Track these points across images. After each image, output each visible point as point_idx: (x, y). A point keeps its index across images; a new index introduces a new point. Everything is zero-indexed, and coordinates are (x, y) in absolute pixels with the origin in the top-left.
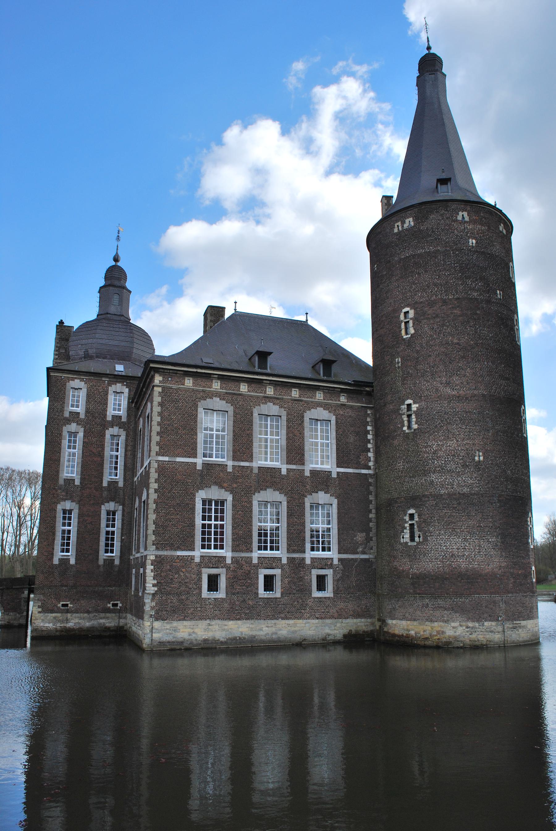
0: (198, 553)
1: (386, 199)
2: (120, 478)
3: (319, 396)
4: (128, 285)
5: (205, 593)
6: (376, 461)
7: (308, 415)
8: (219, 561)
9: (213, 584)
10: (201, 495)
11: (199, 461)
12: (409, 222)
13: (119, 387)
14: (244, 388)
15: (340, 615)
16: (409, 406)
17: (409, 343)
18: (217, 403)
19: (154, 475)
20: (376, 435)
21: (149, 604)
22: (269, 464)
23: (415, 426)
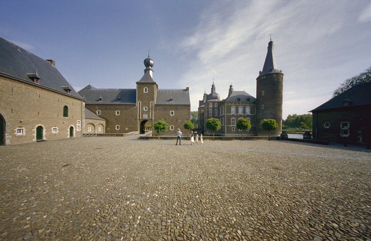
0: (231, 126)
1: (260, 72)
2: (217, 115)
3: (248, 104)
4: (215, 87)
5: (232, 130)
6: (256, 113)
7: (246, 107)
8: (234, 127)
9: (233, 129)
10: (232, 118)
11: (231, 114)
12: (265, 77)
13: (216, 103)
14: (237, 104)
15: (250, 133)
16: (263, 106)
17: (263, 96)
18: (234, 106)
19: (226, 116)
20: (256, 109)
21: (226, 132)
22: (241, 114)
23: (263, 108)
